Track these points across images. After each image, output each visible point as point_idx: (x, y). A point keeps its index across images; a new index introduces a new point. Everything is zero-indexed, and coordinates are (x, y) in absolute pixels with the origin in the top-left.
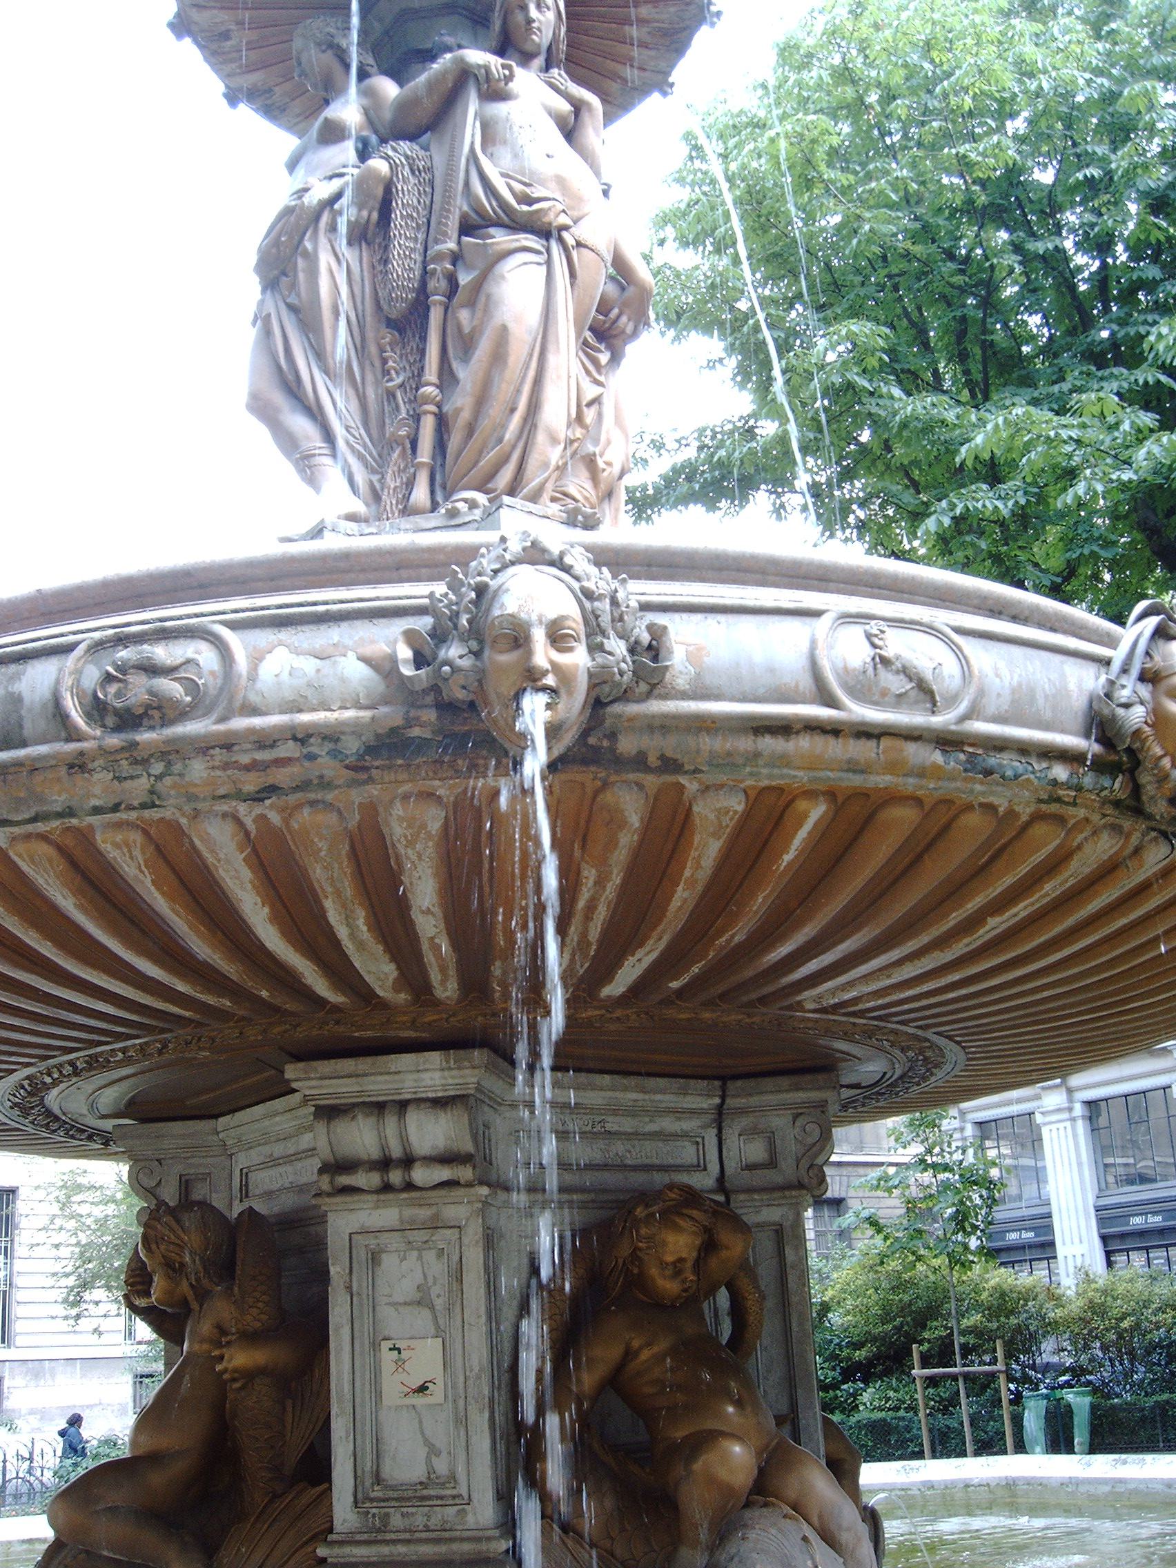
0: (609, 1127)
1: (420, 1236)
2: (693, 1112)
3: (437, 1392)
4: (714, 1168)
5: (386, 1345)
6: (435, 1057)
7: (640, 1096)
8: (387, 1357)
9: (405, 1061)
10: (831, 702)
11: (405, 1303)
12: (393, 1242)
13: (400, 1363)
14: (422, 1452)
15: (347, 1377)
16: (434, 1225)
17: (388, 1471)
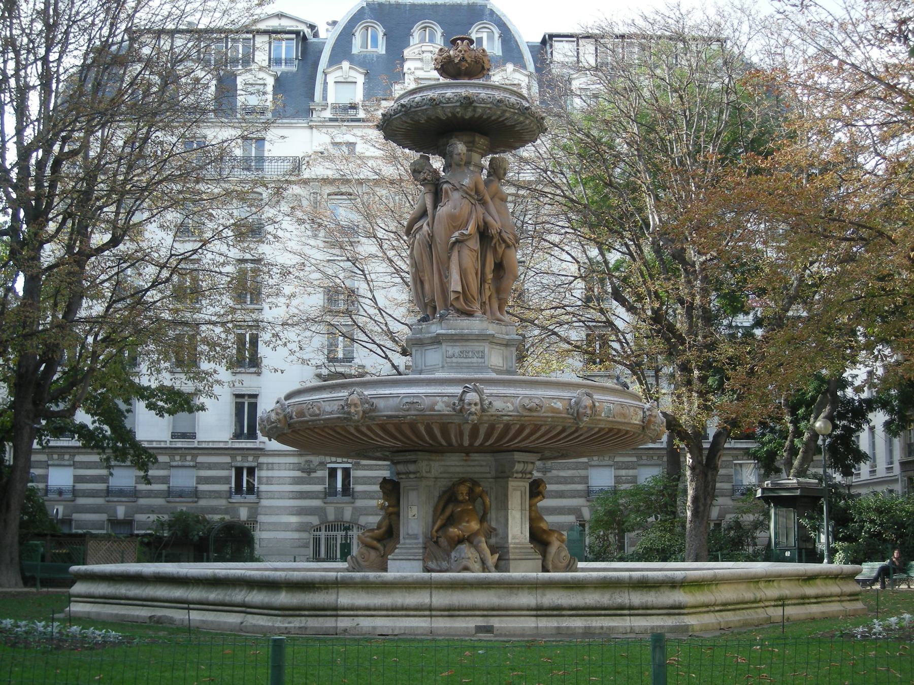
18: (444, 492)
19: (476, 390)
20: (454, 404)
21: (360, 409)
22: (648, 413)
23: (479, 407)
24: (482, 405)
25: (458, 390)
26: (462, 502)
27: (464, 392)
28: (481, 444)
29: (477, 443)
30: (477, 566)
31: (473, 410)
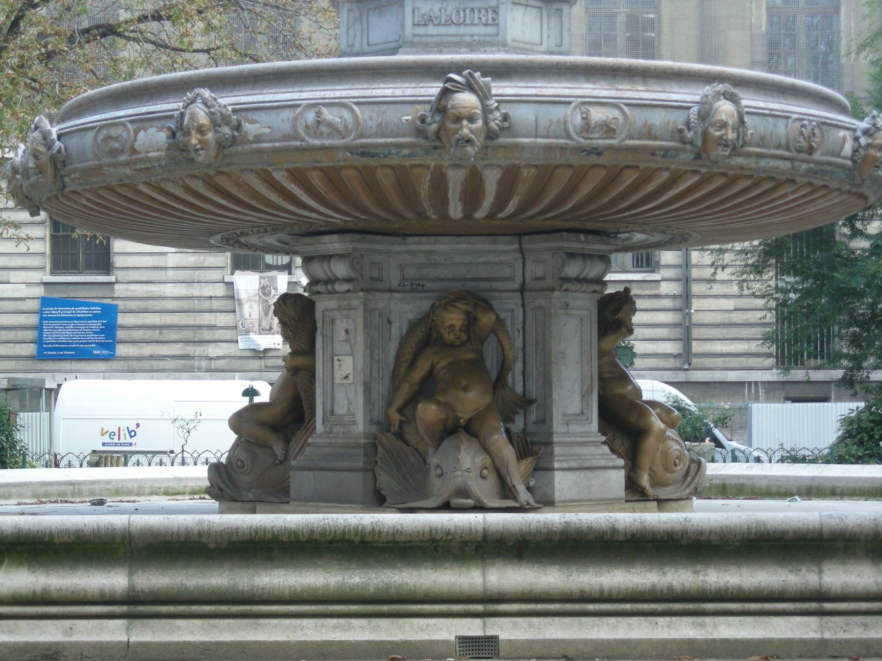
0: (454, 260)
1: (345, 312)
2: (505, 252)
3: (351, 377)
4: (519, 280)
5: (336, 358)
6: (335, 237)
7: (469, 246)
8: (336, 363)
9: (327, 238)
10: (303, 140)
11: (343, 341)
12: (337, 315)
13: (340, 365)
14: (346, 403)
15: (321, 371)
16: (350, 308)
17: (335, 412)
18: (413, 326)
19: (470, 87)
20: (423, 120)
21: (210, 136)
22: (863, 141)
23: (480, 123)
24: (486, 122)
25: (432, 89)
26: (452, 345)
27: (445, 93)
28: (491, 216)
29: (480, 214)
30: (485, 489)
31: (466, 131)
